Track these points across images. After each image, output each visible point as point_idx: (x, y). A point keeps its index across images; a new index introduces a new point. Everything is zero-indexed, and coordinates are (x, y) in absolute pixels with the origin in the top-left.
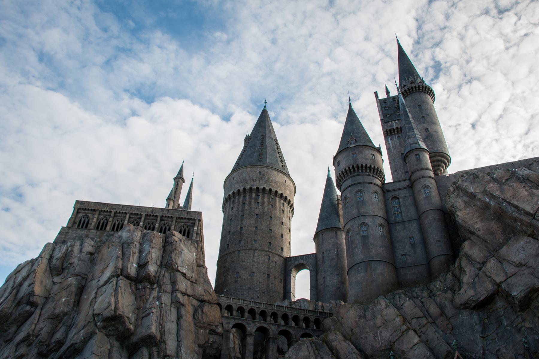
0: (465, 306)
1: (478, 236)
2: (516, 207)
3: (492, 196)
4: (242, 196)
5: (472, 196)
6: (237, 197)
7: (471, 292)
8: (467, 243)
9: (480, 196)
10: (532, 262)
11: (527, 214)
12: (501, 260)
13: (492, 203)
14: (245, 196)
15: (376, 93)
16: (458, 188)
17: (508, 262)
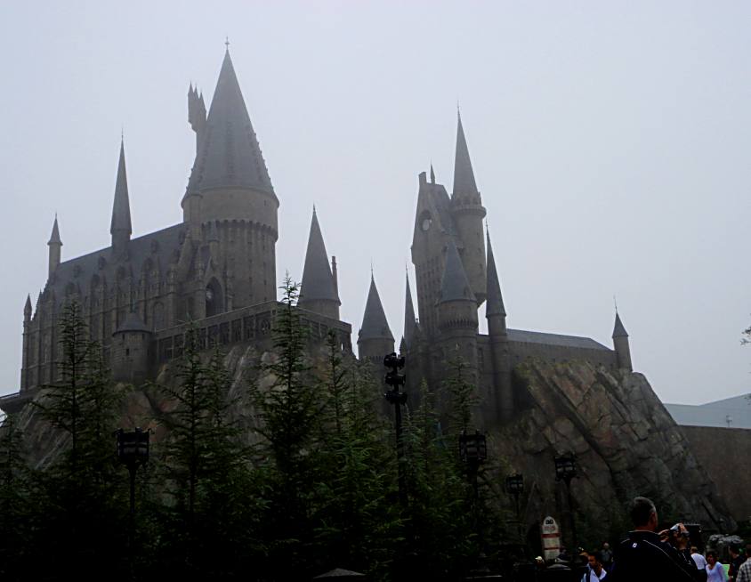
0: (530, 452)
1: (541, 408)
2: (568, 400)
3: (555, 385)
4: (246, 230)
5: (542, 379)
6: (238, 229)
7: (534, 445)
8: (533, 410)
9: (547, 381)
10: (569, 436)
11: (573, 405)
12: (554, 430)
13: (555, 390)
14: (250, 233)
15: (424, 174)
16: (533, 367)
17: (558, 433)
